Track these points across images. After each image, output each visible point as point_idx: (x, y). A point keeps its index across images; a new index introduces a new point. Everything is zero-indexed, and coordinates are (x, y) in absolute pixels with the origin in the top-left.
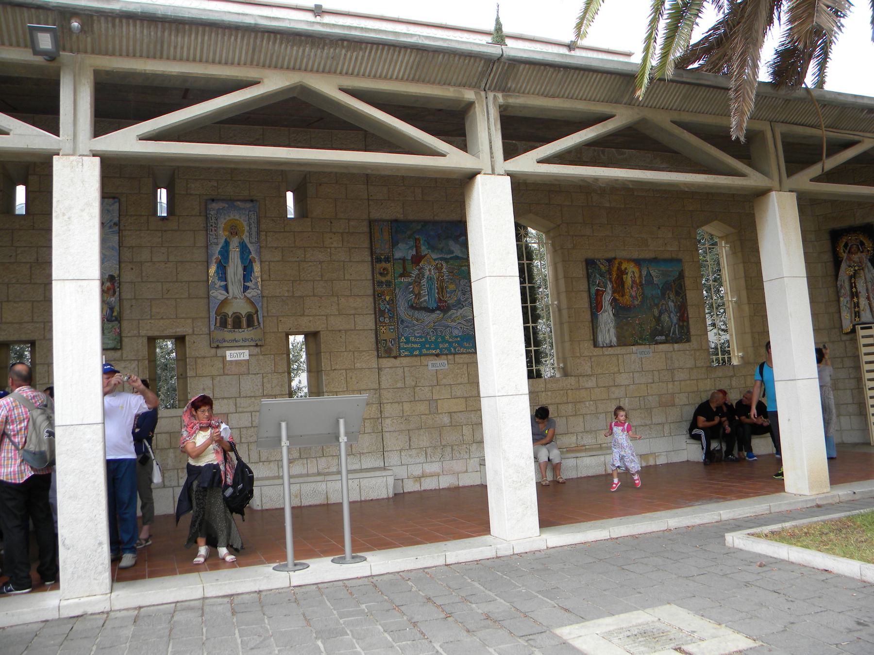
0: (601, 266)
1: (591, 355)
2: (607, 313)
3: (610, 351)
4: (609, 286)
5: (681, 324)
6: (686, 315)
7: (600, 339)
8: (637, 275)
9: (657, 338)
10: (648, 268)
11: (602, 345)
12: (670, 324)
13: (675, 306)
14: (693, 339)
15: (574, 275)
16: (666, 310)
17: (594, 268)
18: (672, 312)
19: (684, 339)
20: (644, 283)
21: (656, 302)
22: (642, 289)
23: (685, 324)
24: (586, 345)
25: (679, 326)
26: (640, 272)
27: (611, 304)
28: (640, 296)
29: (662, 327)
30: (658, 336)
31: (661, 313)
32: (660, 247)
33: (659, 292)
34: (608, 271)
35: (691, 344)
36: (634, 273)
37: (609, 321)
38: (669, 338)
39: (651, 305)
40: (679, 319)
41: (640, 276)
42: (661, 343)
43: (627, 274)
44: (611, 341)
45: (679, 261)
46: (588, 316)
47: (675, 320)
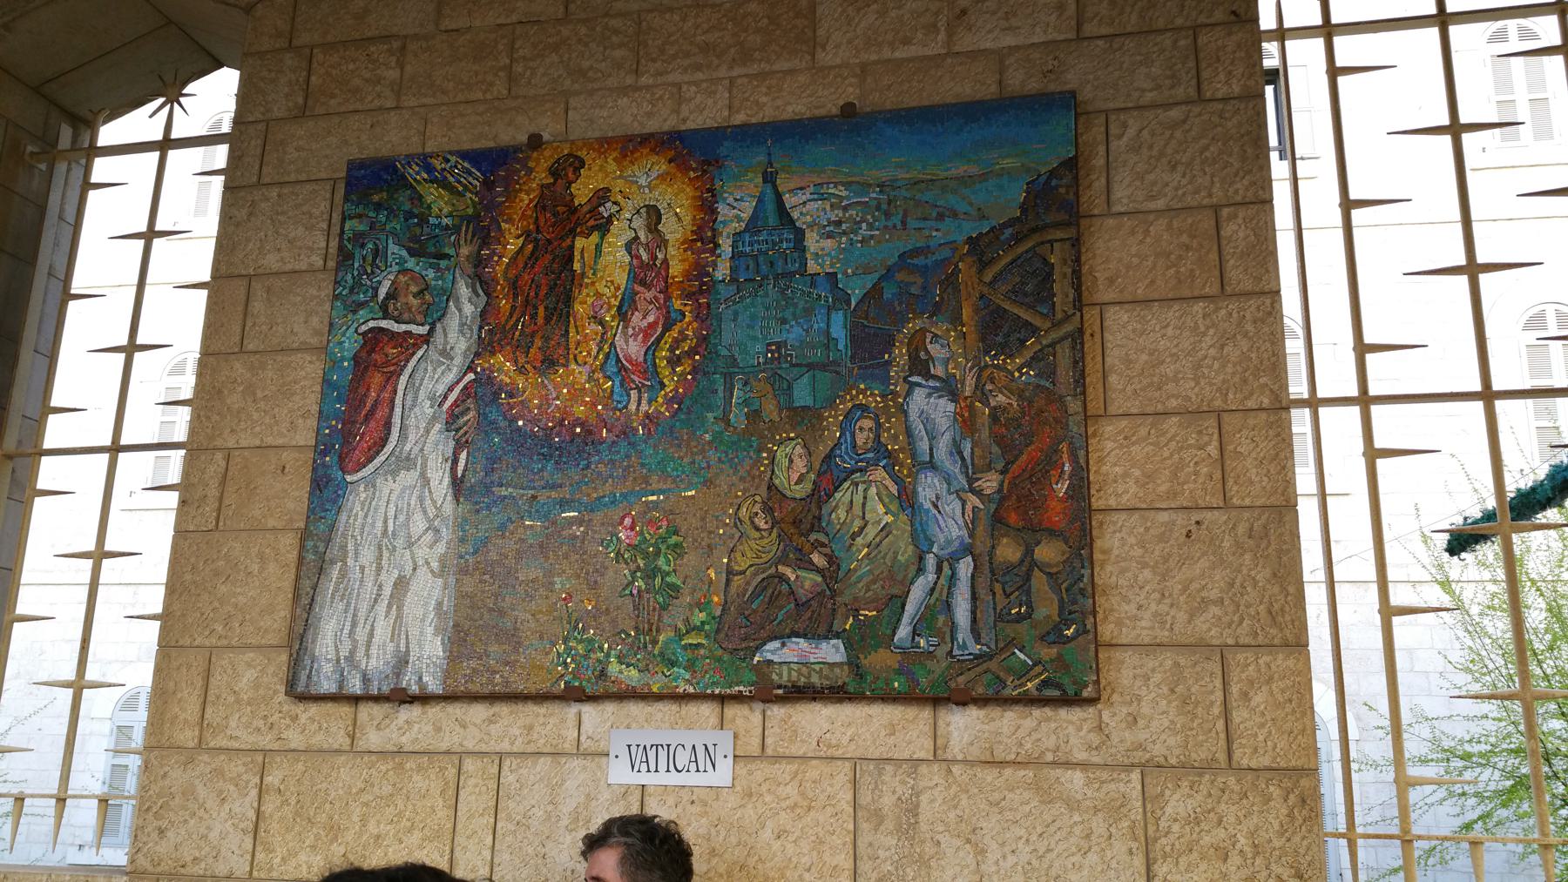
0: (434, 196)
1: (266, 741)
2: (408, 478)
3: (412, 726)
4: (466, 305)
5: (1009, 551)
6: (1062, 488)
7: (328, 640)
8: (674, 230)
9: (772, 651)
10: (769, 178)
11: (328, 686)
12: (906, 553)
13: (966, 423)
14: (1124, 671)
15: (271, 261)
16: (878, 446)
17: (378, 207)
18: (932, 465)
19: (1023, 673)
20: (722, 271)
21: (802, 395)
22: (704, 315)
23: (1048, 552)
24: (250, 675)
25: (990, 573)
26: (707, 207)
27: (452, 419)
28: (674, 362)
29: (833, 572)
30: (783, 636)
31: (829, 479)
32: (906, 42)
33: (839, 331)
34: (476, 218)
35: (1112, 715)
36: (654, 215)
37: (419, 524)
38: (880, 660)
39: (754, 416)
40: (997, 520)
41: (704, 236)
42: (799, 693)
43: (604, 227)
44: (402, 662)
45: (1068, 101)
46: (296, 496)
47: (950, 526)
